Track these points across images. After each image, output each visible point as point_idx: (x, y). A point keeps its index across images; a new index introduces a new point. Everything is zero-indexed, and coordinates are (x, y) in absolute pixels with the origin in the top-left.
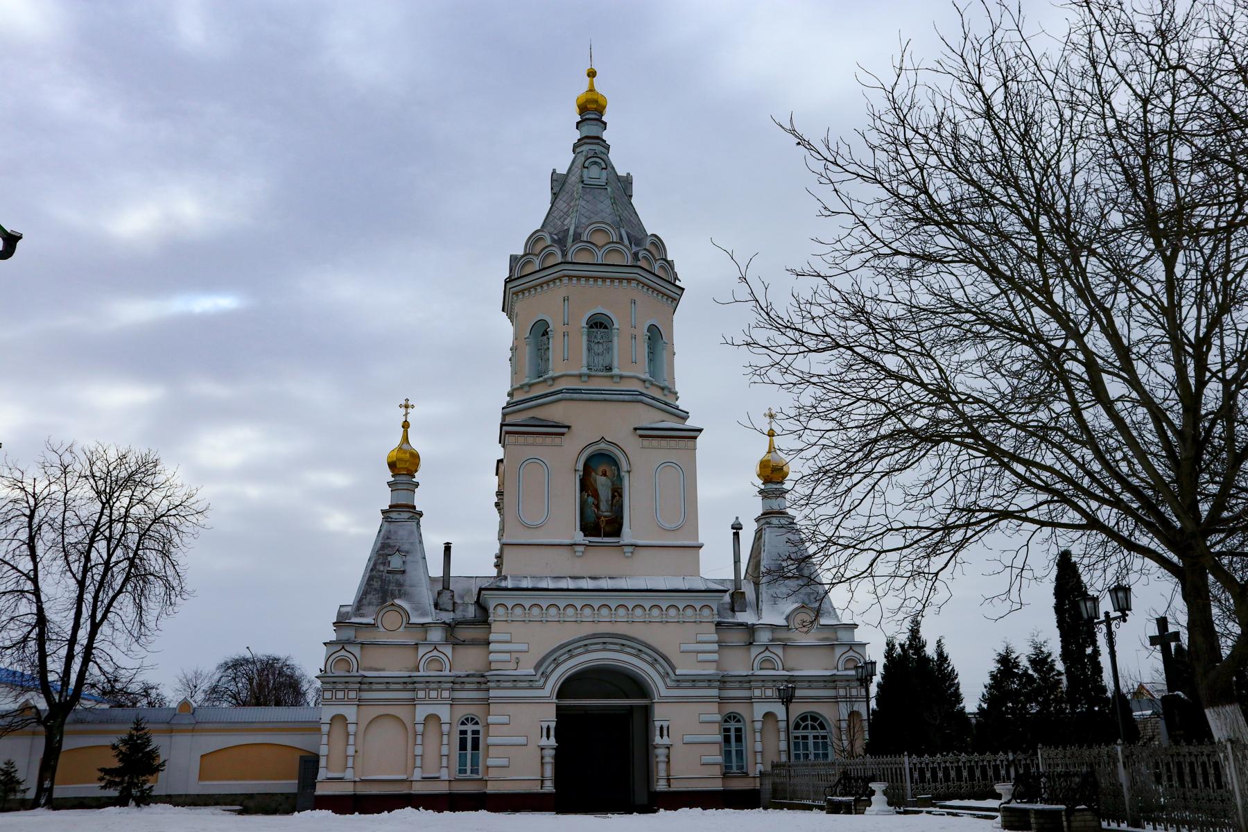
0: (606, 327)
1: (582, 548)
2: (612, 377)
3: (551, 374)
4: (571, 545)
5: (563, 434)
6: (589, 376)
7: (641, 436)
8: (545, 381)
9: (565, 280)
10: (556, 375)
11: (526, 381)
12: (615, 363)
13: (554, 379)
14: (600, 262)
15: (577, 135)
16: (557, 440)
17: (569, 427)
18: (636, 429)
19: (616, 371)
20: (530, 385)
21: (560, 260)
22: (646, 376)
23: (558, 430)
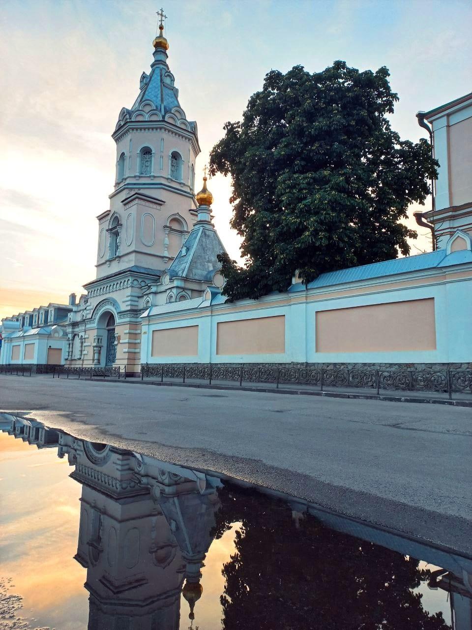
0: (176, 159)
1: (167, 259)
2: (180, 183)
3: (152, 174)
4: (163, 257)
5: (161, 205)
6: (172, 180)
7: (192, 214)
8: (150, 177)
9: (163, 130)
10: (155, 175)
11: (138, 174)
12: (182, 178)
13: (154, 177)
14: (178, 125)
15: (152, 60)
16: (158, 207)
17: (164, 202)
18: (190, 210)
19: (182, 181)
20: (140, 177)
21: (161, 119)
22: (191, 187)
23: (159, 203)
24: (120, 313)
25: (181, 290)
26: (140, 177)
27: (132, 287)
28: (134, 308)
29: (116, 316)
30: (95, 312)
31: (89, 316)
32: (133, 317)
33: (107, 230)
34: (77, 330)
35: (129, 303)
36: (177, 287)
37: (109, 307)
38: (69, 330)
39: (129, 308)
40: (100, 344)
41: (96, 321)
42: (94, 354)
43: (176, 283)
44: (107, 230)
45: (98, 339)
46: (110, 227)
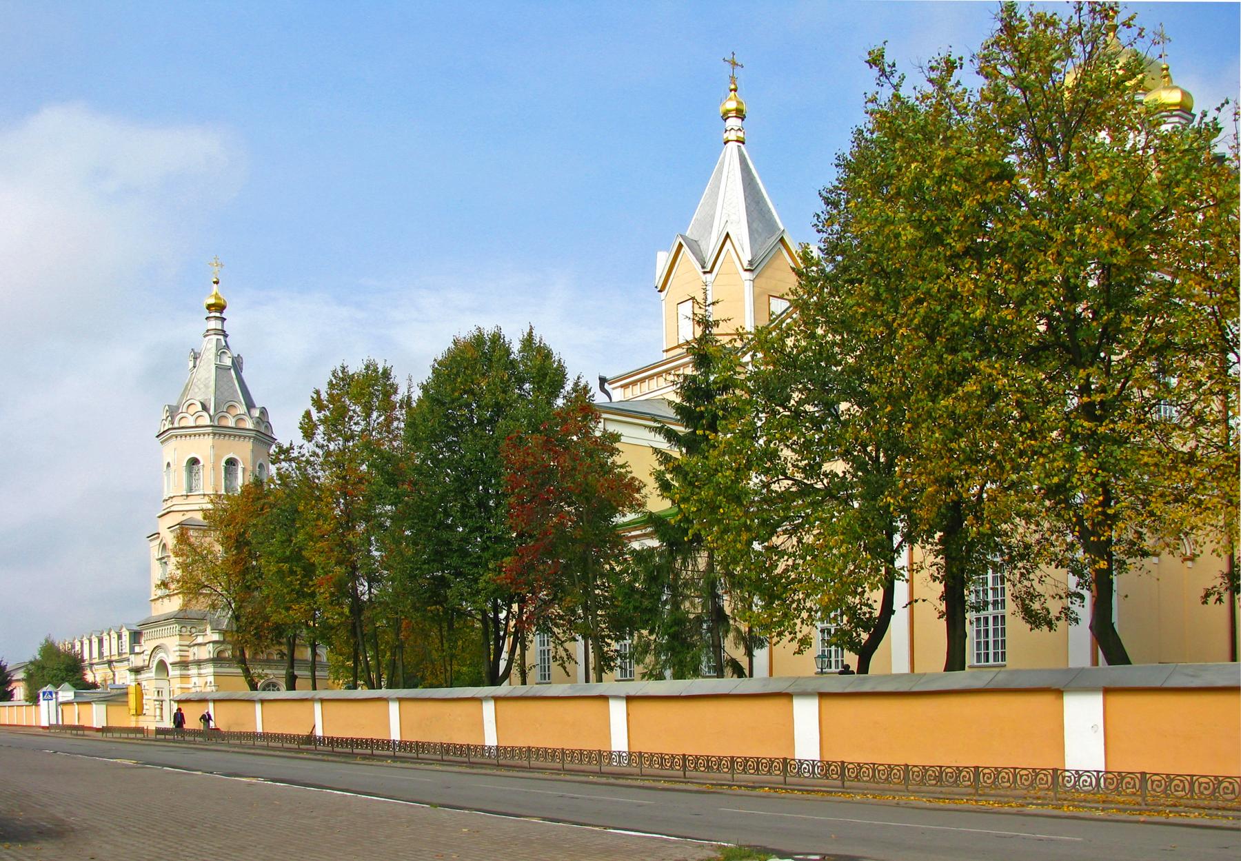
3: (201, 492)
20: (187, 496)
24: (173, 664)
25: (216, 646)
26: (187, 496)
27: (180, 635)
28: (184, 659)
29: (170, 667)
30: (152, 659)
31: (147, 663)
32: (184, 669)
33: (157, 560)
34: (139, 677)
35: (178, 653)
36: (214, 642)
37: (161, 655)
38: (133, 677)
39: (178, 659)
40: (160, 698)
41: (154, 669)
42: (155, 709)
43: (216, 637)
44: (157, 560)
45: (158, 692)
46: (160, 557)
